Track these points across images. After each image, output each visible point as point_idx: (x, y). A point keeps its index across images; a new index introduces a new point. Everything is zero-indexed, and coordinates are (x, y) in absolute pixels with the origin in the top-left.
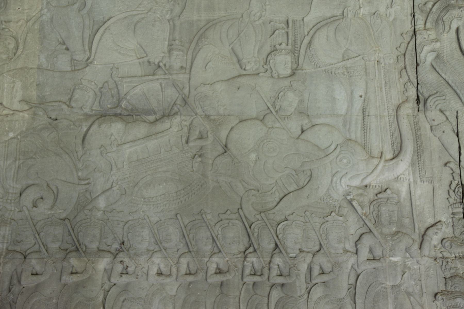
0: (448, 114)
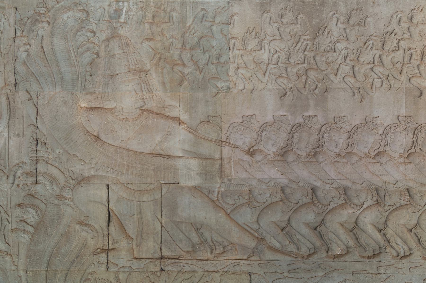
0: (32, 93)
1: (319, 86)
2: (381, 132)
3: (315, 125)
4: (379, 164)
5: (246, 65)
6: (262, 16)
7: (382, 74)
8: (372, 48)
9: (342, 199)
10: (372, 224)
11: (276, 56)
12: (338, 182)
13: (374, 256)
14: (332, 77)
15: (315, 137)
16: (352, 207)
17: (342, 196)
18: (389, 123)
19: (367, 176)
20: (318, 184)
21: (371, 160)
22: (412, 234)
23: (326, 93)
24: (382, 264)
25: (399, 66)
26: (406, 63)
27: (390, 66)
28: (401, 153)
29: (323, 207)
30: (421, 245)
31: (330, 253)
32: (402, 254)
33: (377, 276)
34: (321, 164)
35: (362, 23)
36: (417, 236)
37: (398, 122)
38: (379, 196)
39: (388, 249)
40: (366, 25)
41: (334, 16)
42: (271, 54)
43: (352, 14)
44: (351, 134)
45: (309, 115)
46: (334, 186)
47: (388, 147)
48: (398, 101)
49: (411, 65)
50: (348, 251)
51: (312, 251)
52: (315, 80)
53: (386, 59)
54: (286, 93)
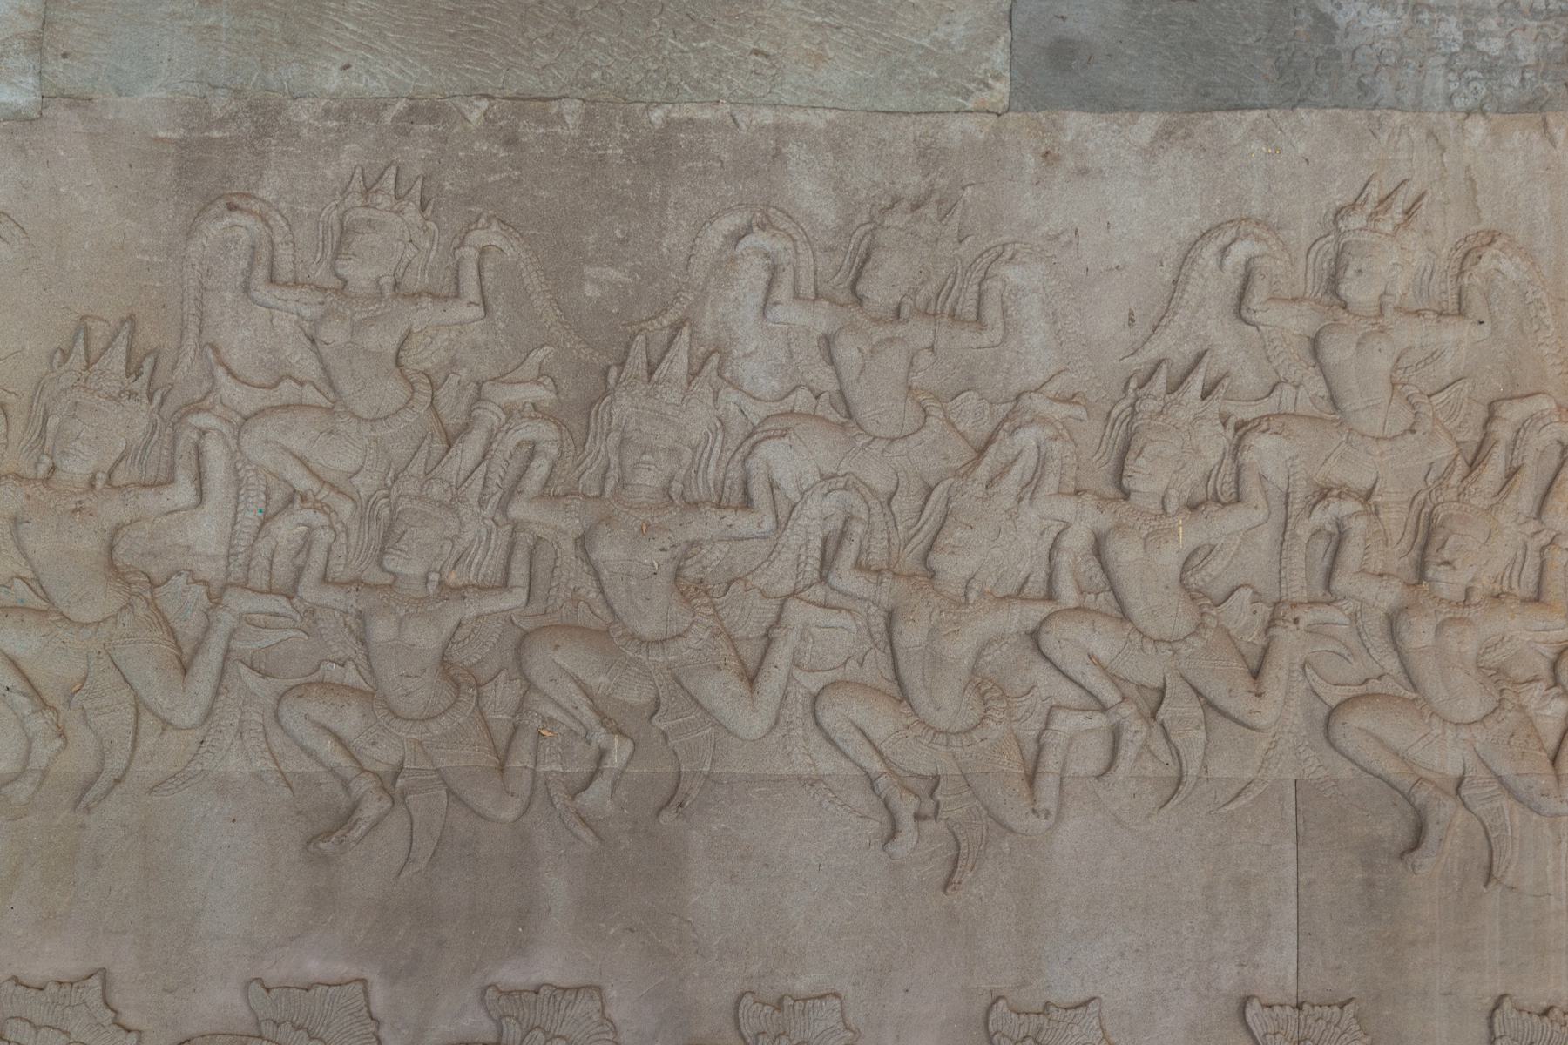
1: (616, 760)
5: (47, 599)
6: (189, 235)
7: (1115, 679)
8: (1032, 485)
11: (286, 530)
14: (721, 691)
23: (667, 817)
25: (1242, 616)
26: (1302, 596)
27: (1174, 617)
35: (959, 304)
40: (992, 313)
41: (748, 241)
42: (250, 518)
43: (882, 236)
45: (535, 979)
53: (1150, 567)
54: (355, 808)
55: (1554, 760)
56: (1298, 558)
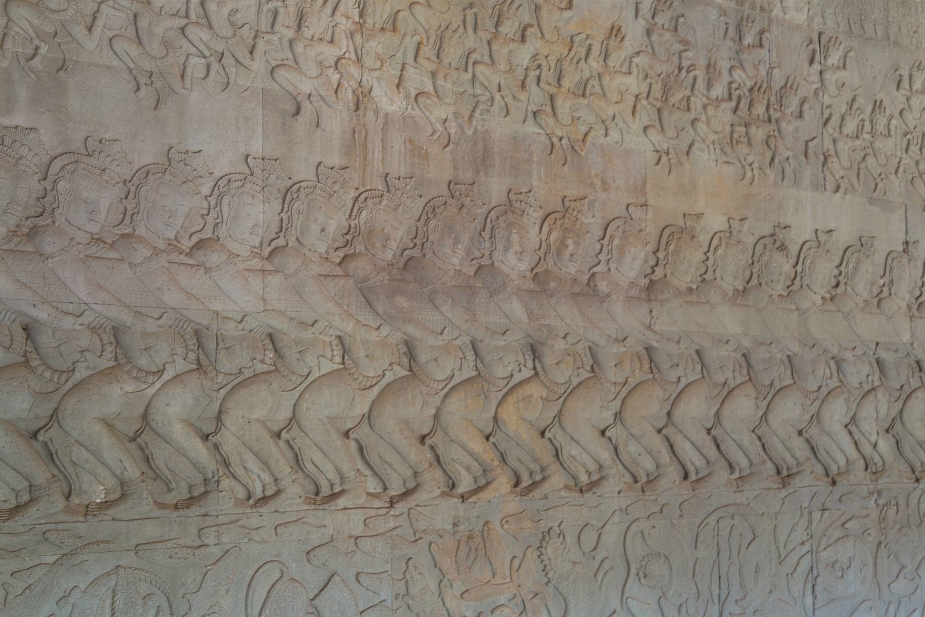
1: (44, 49)
2: (206, 190)
3: (31, 154)
4: (202, 271)
9: (108, 355)
10: (185, 421)
12: (95, 312)
13: (191, 501)
14: (79, 32)
15: (33, 185)
16: (135, 378)
17: (109, 348)
18: (226, 170)
19: (173, 298)
20: (42, 314)
21: (183, 258)
22: (281, 443)
23: (61, 73)
24: (209, 521)
25: (247, 33)
26: (264, 30)
27: (227, 31)
28: (255, 247)
29: (56, 376)
30: (301, 469)
31: (75, 500)
32: (259, 494)
33: (197, 552)
34: (50, 261)
36: (291, 448)
37: (247, 171)
38: (203, 350)
39: (226, 483)
44: (132, 188)
45: (15, 124)
46: (87, 322)
47: (224, 228)
48: (247, 119)
49: (275, 38)
50: (124, 492)
51: (25, 498)
52: (32, 34)
55: (336, 92)
56: (264, 18)
